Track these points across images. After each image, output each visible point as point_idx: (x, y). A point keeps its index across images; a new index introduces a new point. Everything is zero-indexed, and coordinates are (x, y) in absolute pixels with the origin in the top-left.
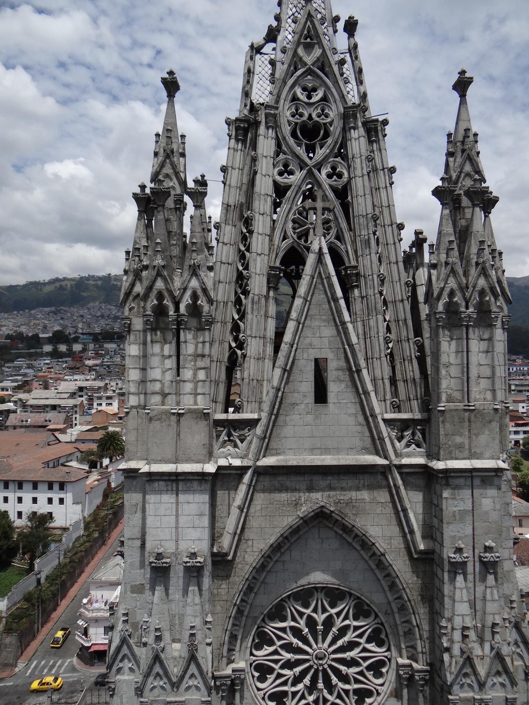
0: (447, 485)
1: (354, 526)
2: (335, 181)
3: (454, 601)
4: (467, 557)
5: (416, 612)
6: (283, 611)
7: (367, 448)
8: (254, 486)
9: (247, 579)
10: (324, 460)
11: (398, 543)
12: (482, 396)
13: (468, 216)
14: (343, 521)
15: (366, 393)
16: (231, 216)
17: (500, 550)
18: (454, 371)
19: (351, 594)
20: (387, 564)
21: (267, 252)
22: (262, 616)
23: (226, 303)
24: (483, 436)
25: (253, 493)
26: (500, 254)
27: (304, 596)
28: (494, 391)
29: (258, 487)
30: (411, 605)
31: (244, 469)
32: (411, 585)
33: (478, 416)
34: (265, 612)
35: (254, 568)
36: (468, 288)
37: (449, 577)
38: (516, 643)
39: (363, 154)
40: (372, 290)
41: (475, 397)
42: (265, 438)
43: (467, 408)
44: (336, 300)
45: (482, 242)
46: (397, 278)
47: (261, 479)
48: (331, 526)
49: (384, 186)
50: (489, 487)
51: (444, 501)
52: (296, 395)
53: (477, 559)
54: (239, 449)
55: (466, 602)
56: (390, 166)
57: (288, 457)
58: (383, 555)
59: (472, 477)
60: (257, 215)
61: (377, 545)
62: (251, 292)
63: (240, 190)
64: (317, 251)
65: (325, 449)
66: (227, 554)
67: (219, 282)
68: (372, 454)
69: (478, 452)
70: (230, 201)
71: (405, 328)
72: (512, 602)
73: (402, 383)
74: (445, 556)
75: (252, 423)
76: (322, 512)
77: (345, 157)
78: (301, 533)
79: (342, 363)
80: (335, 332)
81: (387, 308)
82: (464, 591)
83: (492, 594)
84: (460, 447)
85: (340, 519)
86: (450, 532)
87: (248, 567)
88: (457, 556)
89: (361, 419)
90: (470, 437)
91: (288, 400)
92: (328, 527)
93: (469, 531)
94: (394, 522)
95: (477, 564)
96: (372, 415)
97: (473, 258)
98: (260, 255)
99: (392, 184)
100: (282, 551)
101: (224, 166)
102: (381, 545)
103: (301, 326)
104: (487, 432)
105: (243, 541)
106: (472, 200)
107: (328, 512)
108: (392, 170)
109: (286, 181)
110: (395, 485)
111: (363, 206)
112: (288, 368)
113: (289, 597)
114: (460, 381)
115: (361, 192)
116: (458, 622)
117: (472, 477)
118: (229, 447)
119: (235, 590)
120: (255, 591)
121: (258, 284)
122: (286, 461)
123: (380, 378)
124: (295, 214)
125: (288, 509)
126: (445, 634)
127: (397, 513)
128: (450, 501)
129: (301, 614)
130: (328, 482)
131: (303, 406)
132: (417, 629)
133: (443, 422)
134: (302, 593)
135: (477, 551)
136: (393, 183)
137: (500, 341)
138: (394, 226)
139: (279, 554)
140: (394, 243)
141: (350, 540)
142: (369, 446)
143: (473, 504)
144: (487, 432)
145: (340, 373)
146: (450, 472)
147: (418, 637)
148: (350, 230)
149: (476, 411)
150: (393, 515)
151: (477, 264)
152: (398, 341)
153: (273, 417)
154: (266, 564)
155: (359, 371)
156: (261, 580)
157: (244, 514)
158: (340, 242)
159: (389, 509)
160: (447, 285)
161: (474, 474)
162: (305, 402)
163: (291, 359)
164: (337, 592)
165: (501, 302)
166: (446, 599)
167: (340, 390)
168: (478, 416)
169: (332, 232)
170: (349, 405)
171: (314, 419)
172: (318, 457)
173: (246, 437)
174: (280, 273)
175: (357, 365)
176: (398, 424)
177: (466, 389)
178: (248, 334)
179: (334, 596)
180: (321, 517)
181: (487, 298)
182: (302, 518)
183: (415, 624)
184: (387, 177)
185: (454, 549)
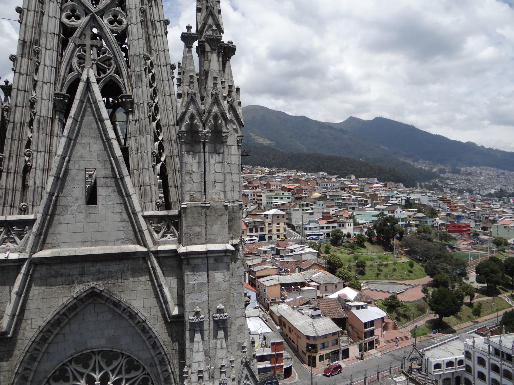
0: (188, 264)
1: (120, 301)
2: (116, 26)
3: (193, 351)
4: (202, 318)
5: (171, 362)
6: (66, 373)
7: (131, 240)
8: (31, 275)
9: (27, 351)
10: (93, 250)
11: (156, 311)
12: (217, 196)
13: (209, 58)
14: (111, 298)
15: (129, 196)
16: (27, 51)
17: (228, 311)
18: (196, 177)
19: (123, 355)
20: (148, 329)
21: (53, 81)
22: (46, 380)
23: (22, 125)
24: (216, 226)
25: (30, 280)
26: (238, 90)
27: (83, 360)
28: (225, 192)
29: (36, 275)
30: (168, 358)
31: (20, 262)
32: (167, 343)
33: (213, 211)
34: (49, 376)
35: (34, 342)
36: (204, 113)
37: (190, 334)
38: (247, 378)
39: (137, 6)
40: (143, 115)
41: (212, 197)
42: (40, 234)
43: (204, 205)
44: (102, 121)
45: (215, 78)
46: (170, 108)
47: (38, 268)
48: (104, 302)
49: (160, 34)
50: (220, 265)
51: (186, 277)
52: (69, 198)
53: (211, 319)
54: (17, 244)
55: (202, 351)
56: (165, 19)
57: (62, 249)
58: (144, 321)
59: (207, 258)
60: (43, 50)
61: (139, 314)
62: (38, 114)
63: (35, 29)
64: (85, 80)
65: (95, 241)
66: (6, 333)
67: (16, 106)
68: (135, 244)
69: (212, 238)
70: (26, 38)
71: (176, 146)
72: (244, 348)
73: (174, 189)
74: (186, 319)
75: (31, 222)
76: (97, 292)
77: (124, 9)
78: (78, 310)
79: (109, 172)
80: (102, 147)
81: (161, 131)
82: (201, 343)
83: (221, 344)
84: (198, 235)
85: (109, 296)
86: (189, 300)
87: (27, 341)
88: (196, 318)
89: (125, 216)
90: (206, 227)
91: (61, 204)
92: (102, 303)
93: (205, 298)
94: (153, 295)
95: (212, 323)
96: (133, 213)
97: (209, 90)
98: (46, 83)
99: (166, 33)
100: (62, 325)
101: (19, 8)
102: (143, 314)
103: (72, 142)
104: (219, 223)
105: (23, 321)
106: (211, 46)
107: (98, 291)
108: (167, 22)
109: (73, 23)
110: (152, 267)
111: (138, 48)
112: (60, 177)
113: (70, 361)
114: (200, 185)
115: (136, 37)
116: (195, 367)
117: (207, 258)
118: (9, 244)
119: (16, 362)
120: (38, 360)
121: (45, 108)
122: (60, 252)
123: (149, 184)
124: (80, 52)
125: (63, 291)
126: (186, 377)
127: (155, 289)
128: (190, 277)
129: (82, 374)
130: (98, 267)
131: (75, 207)
132: (172, 375)
133: (185, 216)
134: (82, 357)
135: (211, 313)
136: (167, 32)
137: (235, 155)
138: (168, 66)
139: (59, 328)
140: (168, 80)
141: (120, 312)
142: (132, 238)
143: (208, 277)
144: (219, 223)
145: (107, 180)
146: (190, 255)
147: (173, 381)
148: (128, 66)
149: (211, 208)
150: (152, 290)
151: (212, 95)
152: (171, 157)
153: (48, 217)
154: (46, 337)
155: (122, 178)
156: (43, 350)
157: (22, 298)
158: (119, 76)
159: (149, 286)
160: (189, 111)
161: (209, 255)
162: (77, 204)
163: (63, 169)
164: (111, 353)
165: (236, 126)
166: (188, 351)
167: (107, 193)
168: (213, 211)
169: (112, 67)
170: (115, 206)
171: (85, 218)
172: (89, 248)
173: (24, 234)
174: (64, 99)
175: (120, 173)
176: (156, 219)
177: (203, 191)
178: (33, 149)
179: (109, 356)
180: (93, 295)
181: (220, 122)
182: (75, 298)
183: (170, 371)
184: (163, 27)
185: (194, 313)
